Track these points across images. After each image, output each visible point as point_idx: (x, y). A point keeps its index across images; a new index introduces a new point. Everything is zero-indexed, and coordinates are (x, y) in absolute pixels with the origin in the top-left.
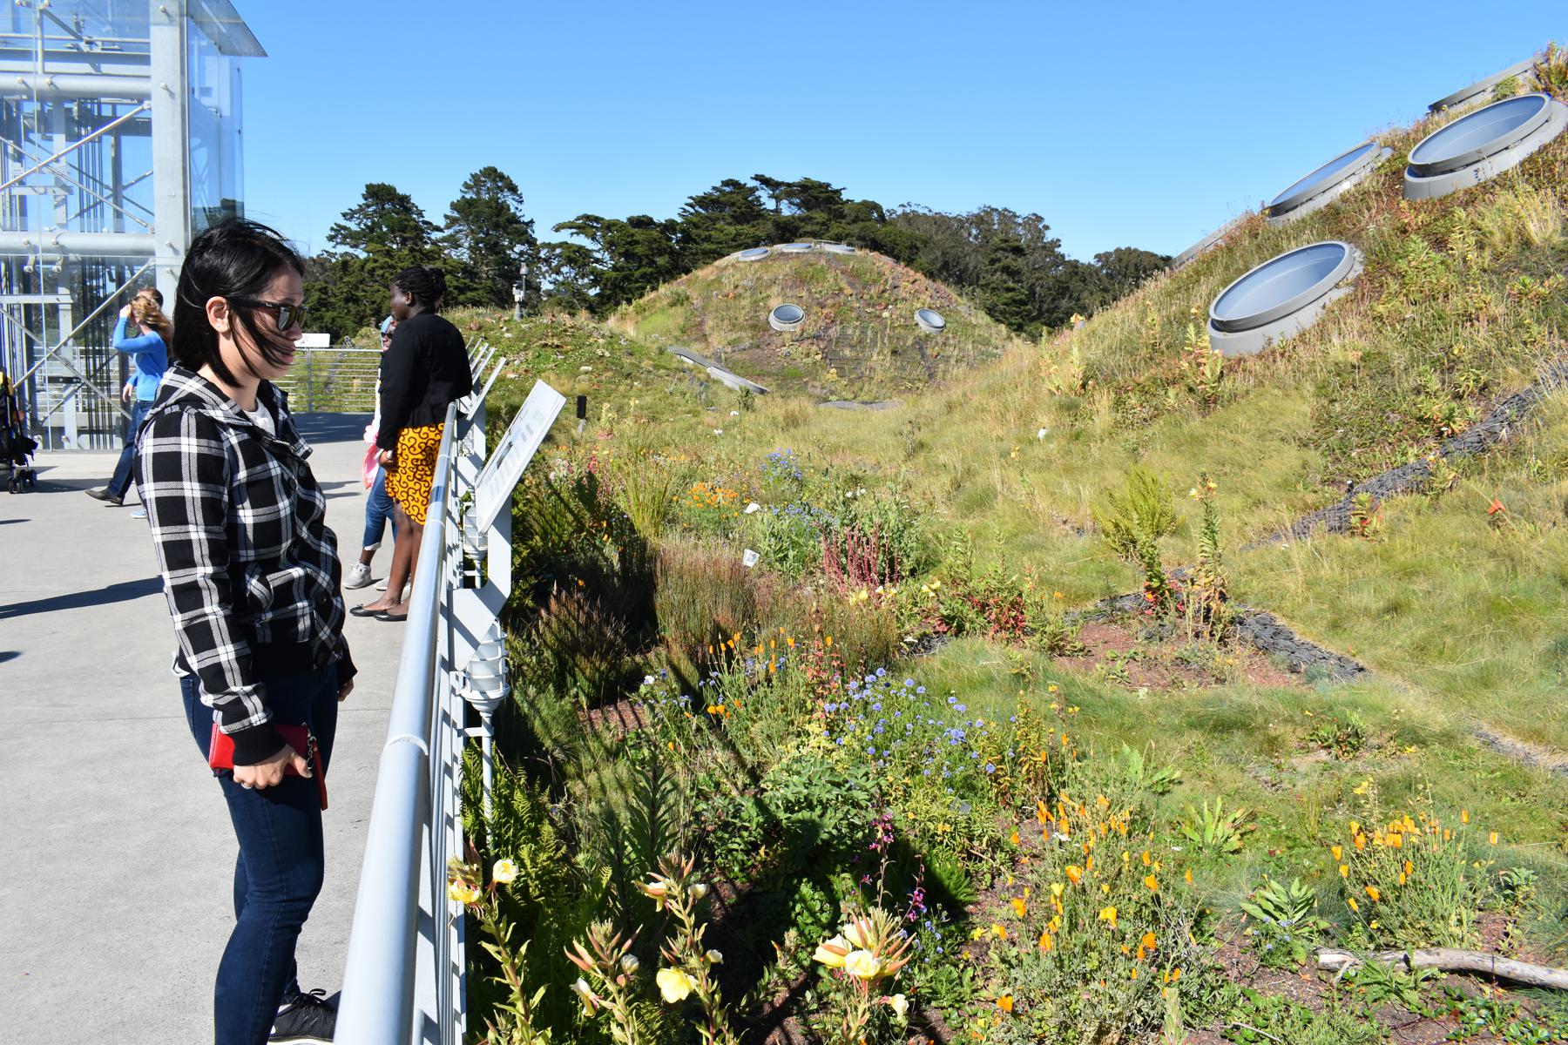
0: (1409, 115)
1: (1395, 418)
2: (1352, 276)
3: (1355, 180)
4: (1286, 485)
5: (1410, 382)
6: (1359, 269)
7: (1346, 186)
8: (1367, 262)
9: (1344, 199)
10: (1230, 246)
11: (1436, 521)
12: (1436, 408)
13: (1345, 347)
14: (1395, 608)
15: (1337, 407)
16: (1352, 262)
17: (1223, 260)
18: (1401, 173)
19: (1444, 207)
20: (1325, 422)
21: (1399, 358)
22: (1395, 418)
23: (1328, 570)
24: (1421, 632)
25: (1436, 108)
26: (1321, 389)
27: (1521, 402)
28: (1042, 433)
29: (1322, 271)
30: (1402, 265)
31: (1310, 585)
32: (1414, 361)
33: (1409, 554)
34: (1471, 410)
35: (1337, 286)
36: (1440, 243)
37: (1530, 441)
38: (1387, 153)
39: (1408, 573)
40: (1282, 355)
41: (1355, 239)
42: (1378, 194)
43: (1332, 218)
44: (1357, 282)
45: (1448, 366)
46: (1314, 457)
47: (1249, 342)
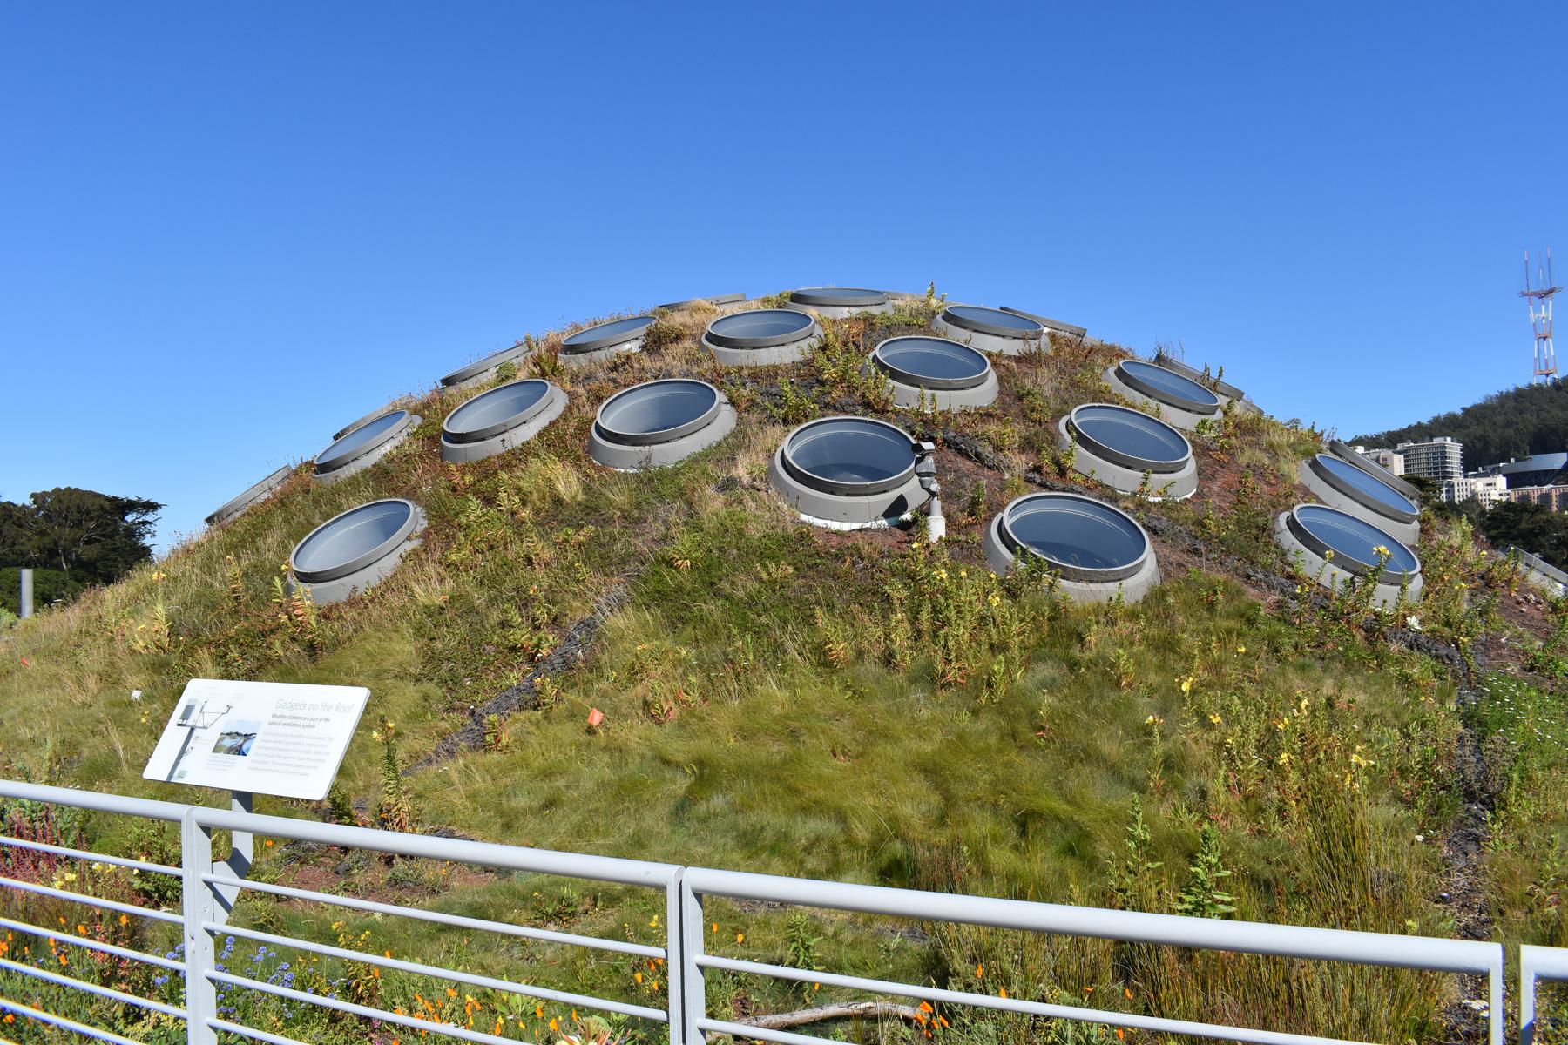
0: (423, 386)
1: (491, 649)
2: (419, 529)
3: (395, 443)
4: (413, 718)
5: (495, 616)
6: (424, 524)
7: (387, 448)
8: (429, 517)
9: (389, 459)
10: (282, 501)
11: (553, 730)
12: (522, 636)
13: (431, 591)
14: (551, 803)
15: (438, 645)
16: (417, 519)
17: (279, 517)
18: (436, 441)
19: (487, 469)
20: (431, 658)
21: (479, 599)
22: (491, 649)
23: (480, 782)
24: (575, 818)
25: (448, 382)
26: (419, 631)
27: (588, 625)
28: (136, 694)
29: (389, 528)
30: (463, 519)
31: (473, 796)
32: (492, 601)
33: (541, 759)
34: (550, 637)
35: (409, 538)
36: (489, 500)
37: (605, 658)
38: (418, 420)
39: (547, 774)
40: (372, 601)
41: (412, 494)
42: (420, 456)
43: (383, 476)
44: (425, 535)
45: (525, 603)
46: (429, 687)
47: (335, 591)
